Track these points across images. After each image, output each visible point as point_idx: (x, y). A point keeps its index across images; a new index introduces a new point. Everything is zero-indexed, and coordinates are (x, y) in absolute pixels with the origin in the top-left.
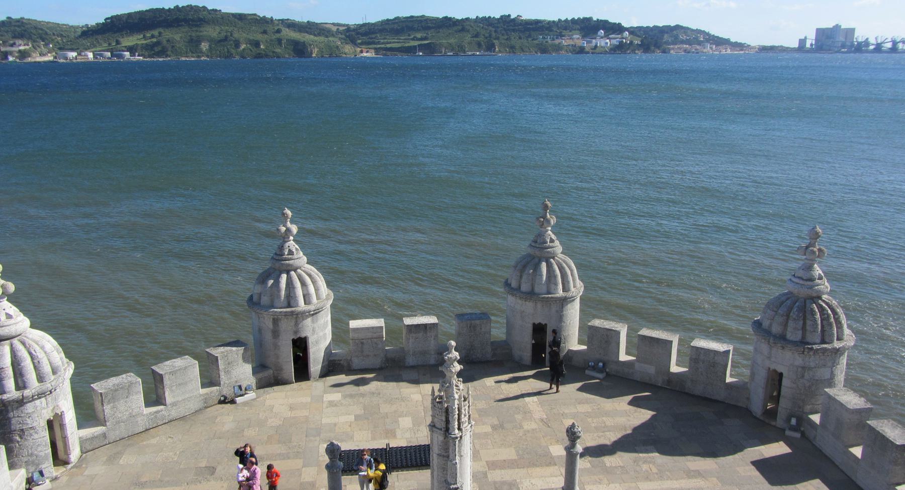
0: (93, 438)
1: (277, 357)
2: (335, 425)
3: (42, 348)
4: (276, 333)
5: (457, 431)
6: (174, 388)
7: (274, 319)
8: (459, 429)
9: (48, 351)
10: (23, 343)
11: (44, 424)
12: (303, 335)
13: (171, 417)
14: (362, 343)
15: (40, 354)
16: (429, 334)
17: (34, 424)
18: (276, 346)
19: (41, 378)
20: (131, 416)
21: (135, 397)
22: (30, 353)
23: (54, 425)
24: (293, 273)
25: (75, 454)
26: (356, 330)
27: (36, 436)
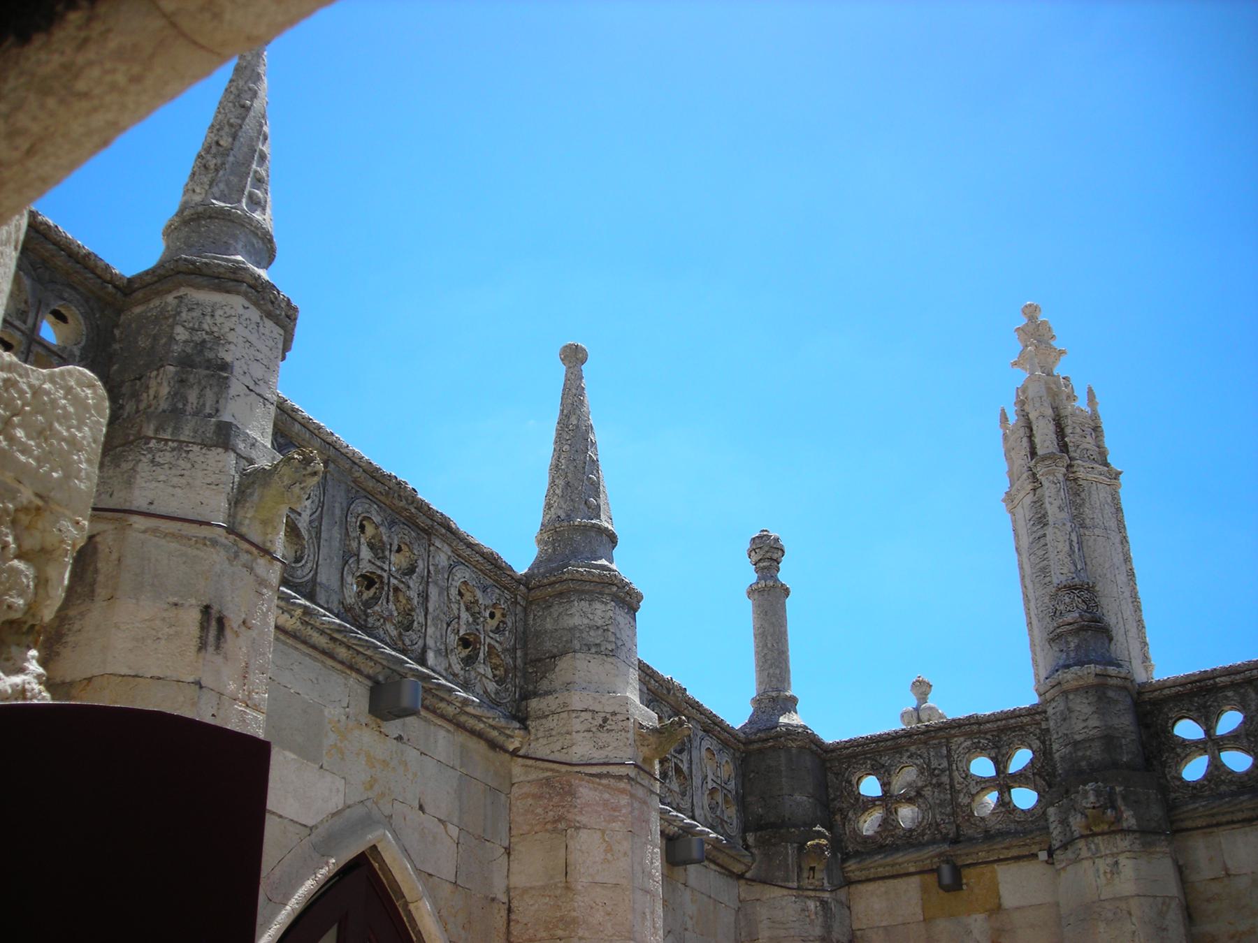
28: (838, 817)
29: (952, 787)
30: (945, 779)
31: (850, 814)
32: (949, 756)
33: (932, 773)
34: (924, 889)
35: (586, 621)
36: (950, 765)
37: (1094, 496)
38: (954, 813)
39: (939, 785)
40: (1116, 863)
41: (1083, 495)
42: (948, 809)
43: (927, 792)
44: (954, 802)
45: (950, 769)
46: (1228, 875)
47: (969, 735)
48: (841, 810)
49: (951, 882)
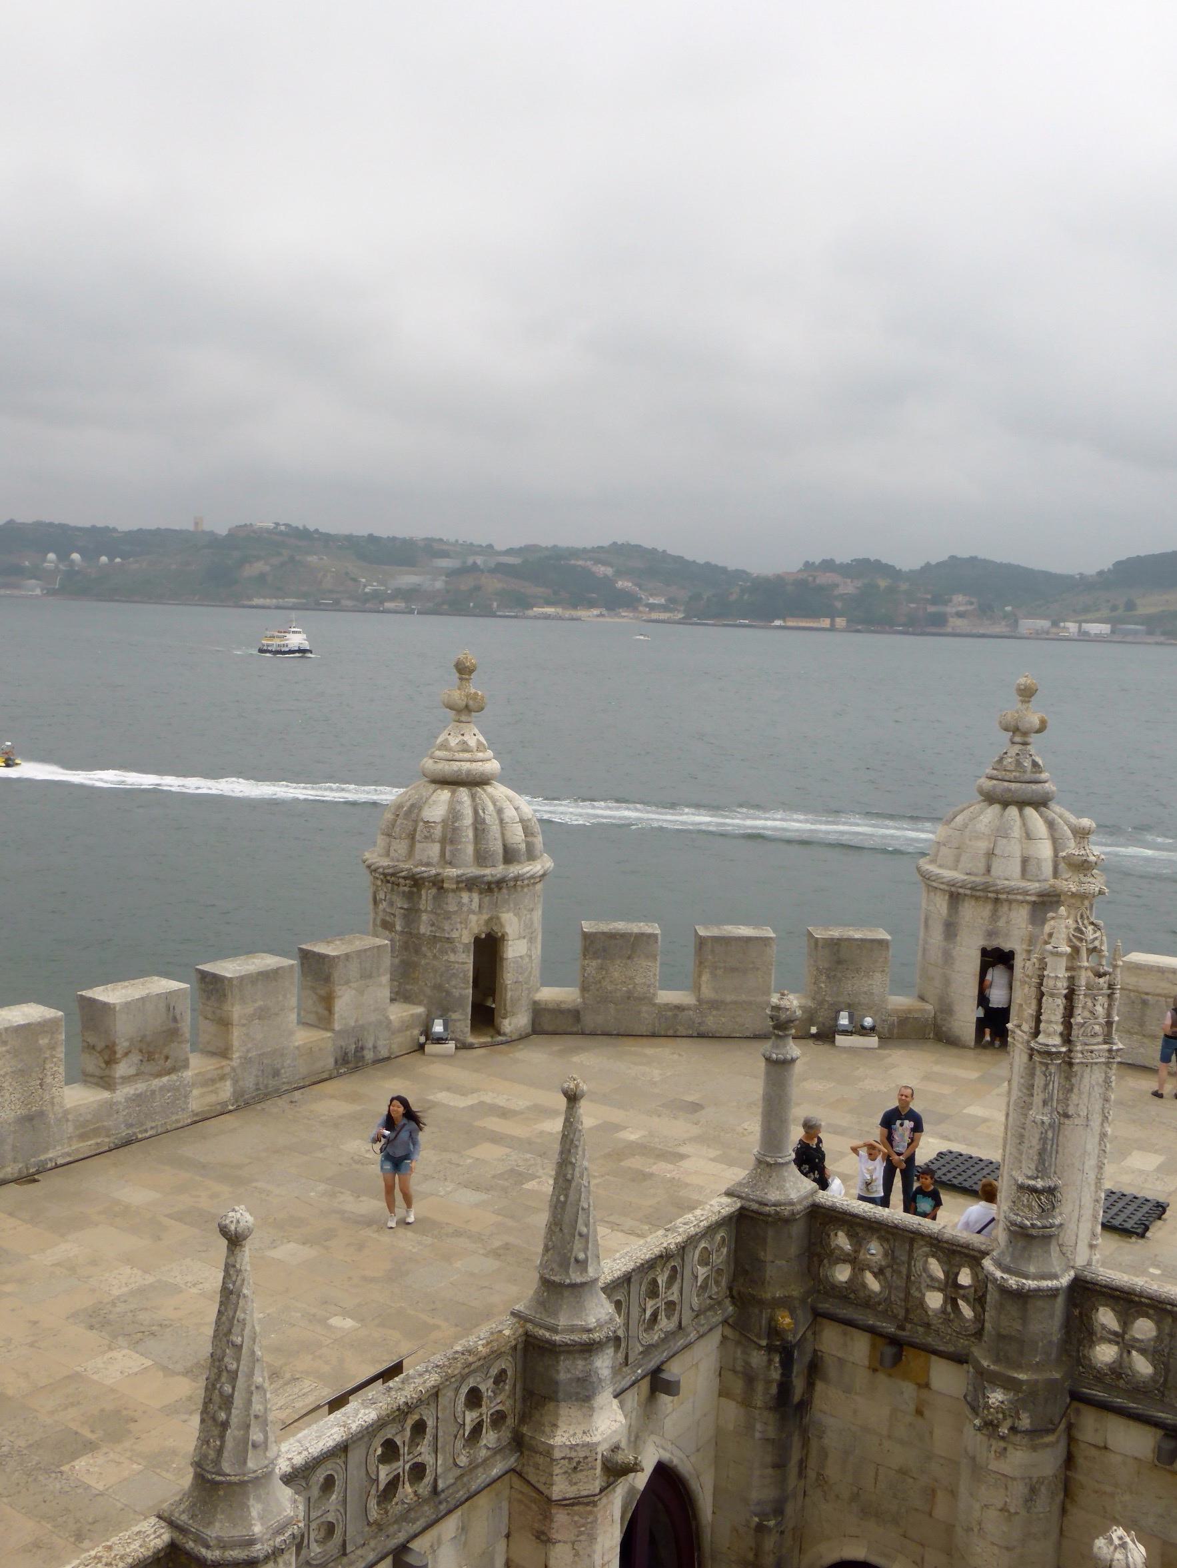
0: (557, 1011)
1: (947, 982)
2: (985, 1120)
3: (500, 811)
4: (951, 929)
5: (1057, 1040)
6: (719, 972)
7: (951, 895)
8: (1067, 1039)
9: (507, 820)
10: (473, 797)
11: (467, 938)
12: (1006, 946)
13: (703, 1029)
14: (1145, 1003)
15: (490, 817)
17: (455, 935)
18: (948, 957)
19: (481, 857)
20: (629, 996)
21: (645, 963)
22: (476, 812)
23: (489, 950)
24: (1013, 811)
25: (515, 1021)
26: (1137, 968)
27: (452, 957)
28: (815, 1259)
29: (908, 1277)
31: (826, 1261)
34: (873, 1346)
35: (569, 1376)
36: (910, 1257)
37: (1086, 1081)
40: (1005, 1449)
41: (1073, 1080)
43: (888, 1272)
44: (908, 1294)
45: (909, 1264)
46: (1106, 1448)
47: (932, 1245)
48: (819, 1255)
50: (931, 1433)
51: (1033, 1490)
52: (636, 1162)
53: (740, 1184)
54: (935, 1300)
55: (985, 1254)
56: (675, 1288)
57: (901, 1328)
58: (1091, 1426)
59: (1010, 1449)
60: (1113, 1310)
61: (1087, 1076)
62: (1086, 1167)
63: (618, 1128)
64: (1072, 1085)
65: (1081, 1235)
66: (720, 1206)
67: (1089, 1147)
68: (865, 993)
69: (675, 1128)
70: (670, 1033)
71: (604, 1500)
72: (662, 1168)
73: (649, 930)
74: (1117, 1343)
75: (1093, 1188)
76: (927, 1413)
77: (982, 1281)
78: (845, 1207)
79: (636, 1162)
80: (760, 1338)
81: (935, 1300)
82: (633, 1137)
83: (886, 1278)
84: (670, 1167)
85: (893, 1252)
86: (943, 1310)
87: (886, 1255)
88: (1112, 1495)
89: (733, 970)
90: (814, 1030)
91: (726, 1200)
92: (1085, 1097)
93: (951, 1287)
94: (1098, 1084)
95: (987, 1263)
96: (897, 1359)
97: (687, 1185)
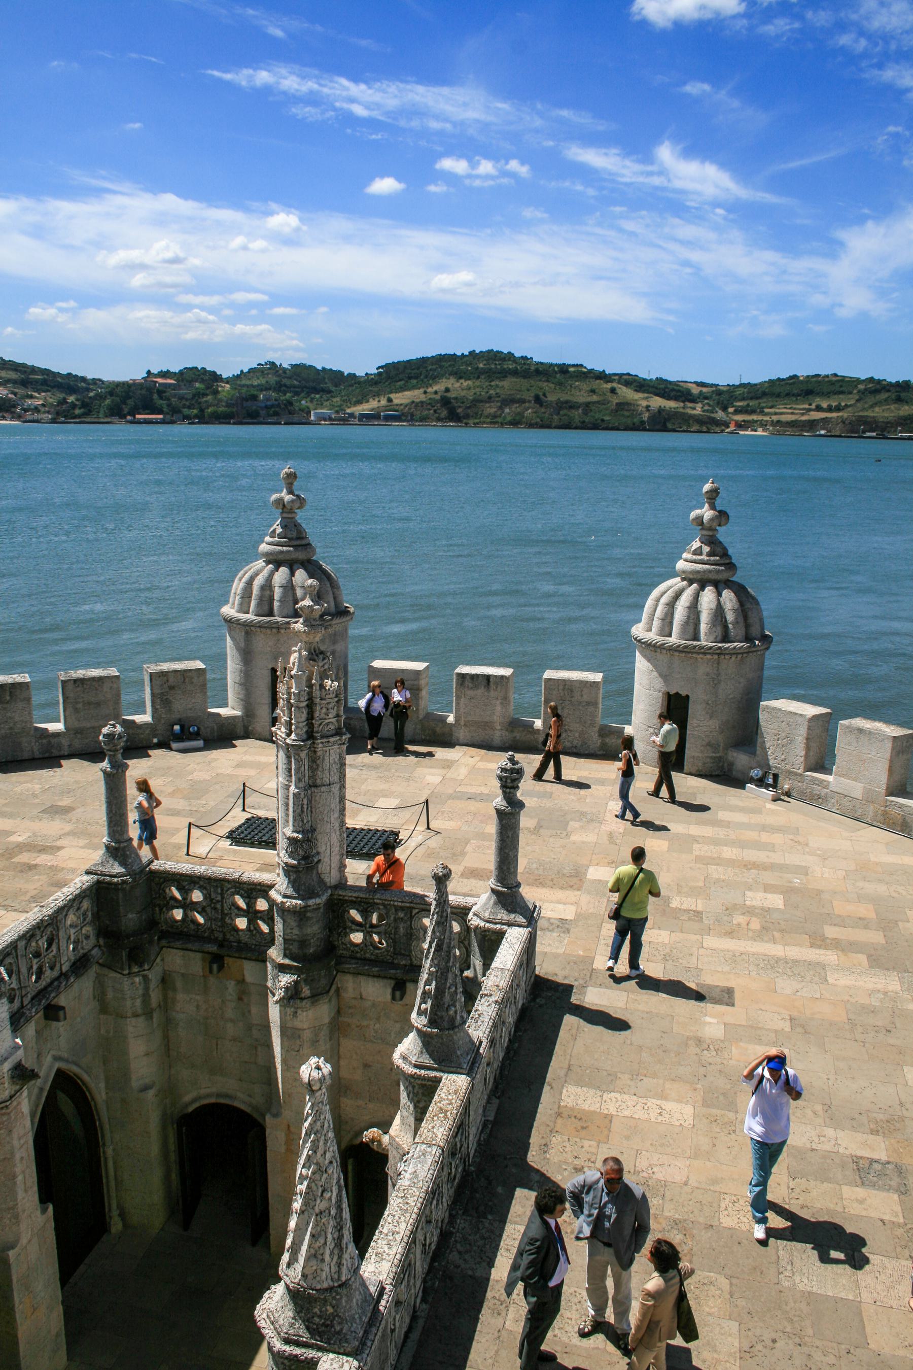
16: (492, 693)
30: (219, 906)
32: (222, 894)
33: (211, 900)
36: (223, 898)
38: (222, 926)
39: (215, 909)
40: (296, 1012)
41: (318, 762)
42: (219, 924)
43: (208, 910)
44: (223, 919)
45: (222, 902)
46: (361, 998)
47: (235, 887)
48: (159, 905)
49: (216, 961)
50: (249, 1012)
51: (316, 1035)
52: (25, 858)
53: (95, 865)
54: (242, 923)
55: (271, 887)
56: (54, 947)
57: (221, 946)
58: (350, 985)
59: (299, 1011)
60: (357, 910)
61: (326, 758)
62: (332, 819)
63: (8, 833)
64: (318, 765)
65: (333, 865)
66: (80, 882)
67: (333, 806)
68: (191, 709)
69: (52, 828)
70: (47, 755)
71: (15, 1103)
72: (43, 859)
73: (22, 680)
74: (362, 931)
75: (338, 833)
76: (246, 1000)
77: (272, 903)
78: (173, 870)
79: (25, 858)
80: (123, 969)
81: (242, 923)
82: (20, 839)
83: (207, 914)
84: (49, 857)
85: (210, 895)
86: (248, 928)
87: (205, 897)
88: (368, 1026)
89: (89, 703)
90: (155, 740)
91: (86, 878)
92: (326, 772)
93: (252, 914)
94: (335, 763)
95: (273, 894)
96: (221, 967)
97: (63, 869)
